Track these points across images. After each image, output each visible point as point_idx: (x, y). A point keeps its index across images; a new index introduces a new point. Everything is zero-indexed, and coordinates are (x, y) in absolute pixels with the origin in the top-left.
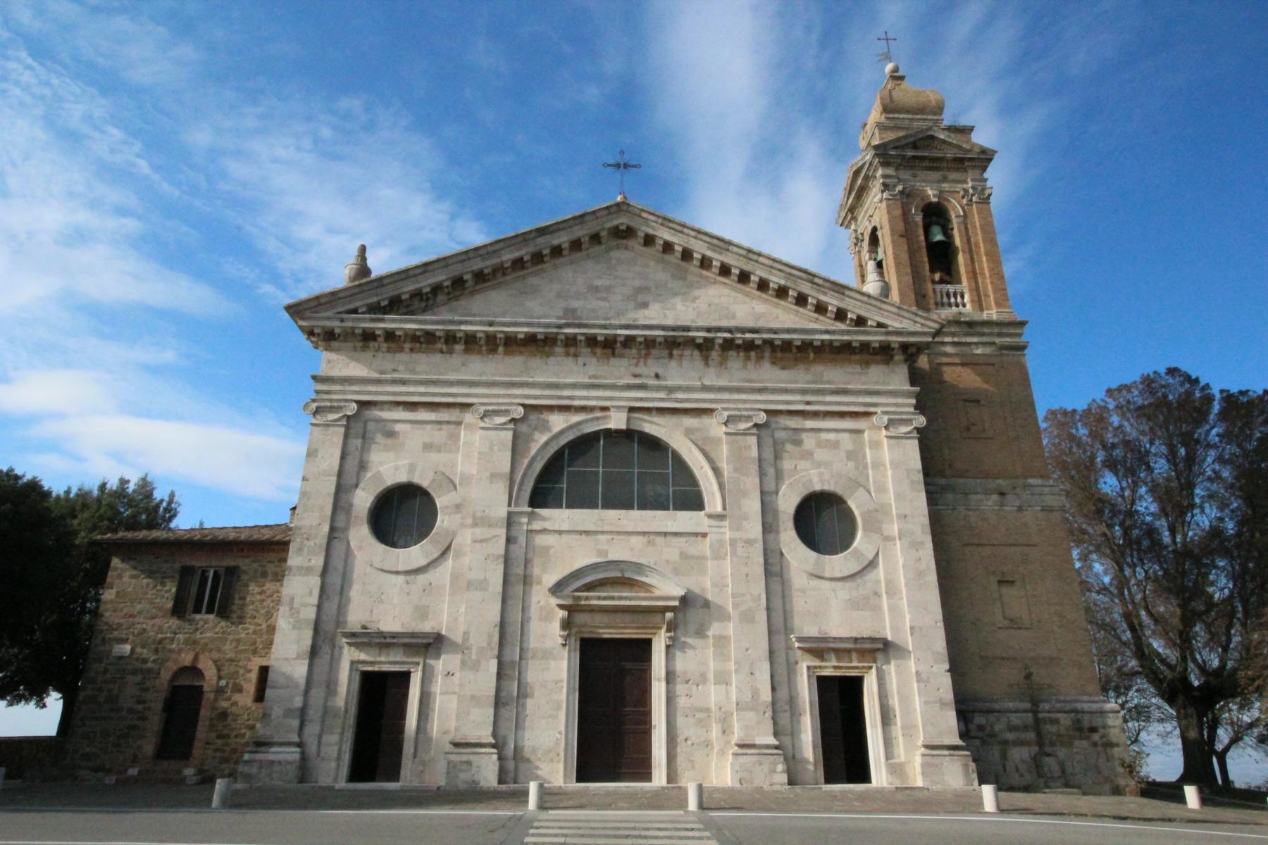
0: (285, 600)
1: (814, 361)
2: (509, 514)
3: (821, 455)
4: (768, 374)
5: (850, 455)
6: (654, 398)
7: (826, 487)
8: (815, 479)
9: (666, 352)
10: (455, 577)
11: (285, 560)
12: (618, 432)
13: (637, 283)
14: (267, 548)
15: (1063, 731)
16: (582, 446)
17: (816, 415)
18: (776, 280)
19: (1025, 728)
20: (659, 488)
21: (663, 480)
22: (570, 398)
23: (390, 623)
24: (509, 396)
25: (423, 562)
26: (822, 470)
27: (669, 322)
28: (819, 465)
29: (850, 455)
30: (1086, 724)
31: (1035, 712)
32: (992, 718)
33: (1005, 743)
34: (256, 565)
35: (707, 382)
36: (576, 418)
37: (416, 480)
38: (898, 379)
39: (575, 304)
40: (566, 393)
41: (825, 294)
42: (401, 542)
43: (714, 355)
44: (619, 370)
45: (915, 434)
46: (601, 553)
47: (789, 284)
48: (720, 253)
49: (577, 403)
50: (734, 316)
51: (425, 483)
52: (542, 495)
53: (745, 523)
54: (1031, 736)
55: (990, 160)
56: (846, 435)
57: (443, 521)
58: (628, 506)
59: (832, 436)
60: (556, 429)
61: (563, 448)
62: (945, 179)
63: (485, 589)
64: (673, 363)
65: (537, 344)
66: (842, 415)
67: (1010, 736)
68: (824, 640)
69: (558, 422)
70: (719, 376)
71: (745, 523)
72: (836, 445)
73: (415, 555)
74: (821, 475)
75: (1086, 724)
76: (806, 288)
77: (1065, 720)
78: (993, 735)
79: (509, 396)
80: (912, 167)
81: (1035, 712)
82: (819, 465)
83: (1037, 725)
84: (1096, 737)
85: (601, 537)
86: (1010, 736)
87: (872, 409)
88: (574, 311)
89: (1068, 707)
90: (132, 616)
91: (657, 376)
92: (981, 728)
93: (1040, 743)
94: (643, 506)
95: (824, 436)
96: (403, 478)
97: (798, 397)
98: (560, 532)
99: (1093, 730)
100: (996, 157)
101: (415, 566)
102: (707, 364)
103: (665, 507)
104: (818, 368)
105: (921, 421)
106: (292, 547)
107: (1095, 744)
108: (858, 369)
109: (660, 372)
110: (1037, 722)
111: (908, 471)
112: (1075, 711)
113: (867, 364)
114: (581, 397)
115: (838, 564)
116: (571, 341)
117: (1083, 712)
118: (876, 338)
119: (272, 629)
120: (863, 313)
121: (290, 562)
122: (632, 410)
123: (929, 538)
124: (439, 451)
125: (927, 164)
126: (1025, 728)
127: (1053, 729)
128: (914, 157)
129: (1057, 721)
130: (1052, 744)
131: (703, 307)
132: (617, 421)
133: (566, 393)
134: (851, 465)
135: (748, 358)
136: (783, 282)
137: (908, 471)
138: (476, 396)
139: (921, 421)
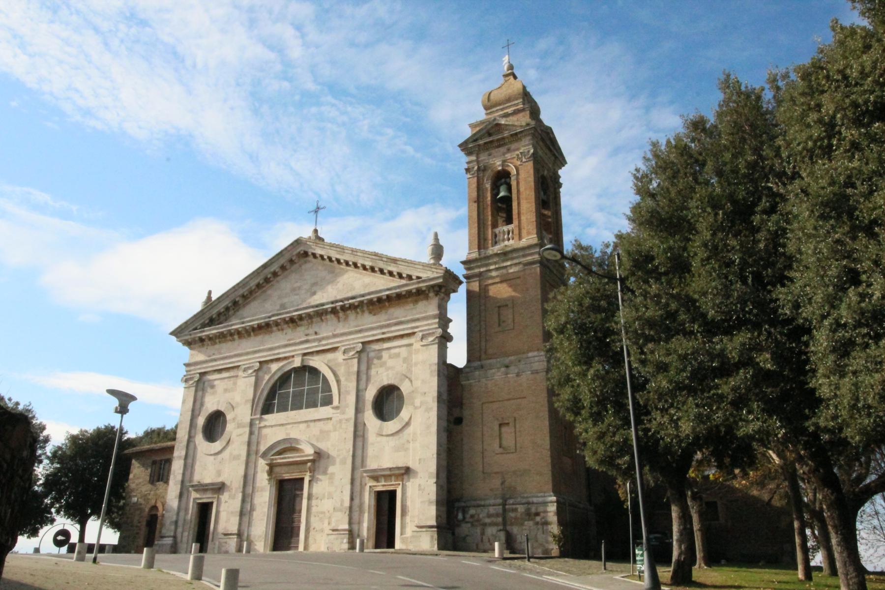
1: (389, 306)
2: (252, 420)
4: (368, 320)
5: (405, 360)
6: (313, 346)
8: (385, 379)
9: (319, 319)
10: (231, 454)
12: (299, 367)
17: (389, 339)
23: (207, 480)
29: (405, 360)
35: (338, 331)
36: (281, 364)
40: (276, 352)
43: (341, 314)
44: (299, 334)
49: (281, 356)
52: (267, 409)
61: (277, 381)
64: (324, 324)
65: (264, 328)
66: (402, 336)
69: (274, 367)
87: (416, 330)
91: (316, 333)
95: (393, 351)
98: (272, 426)
101: (217, 451)
102: (339, 321)
108: (411, 305)
109: (317, 330)
111: (430, 365)
113: (416, 302)
114: (283, 352)
122: (305, 354)
123: (436, 404)
132: (297, 363)
133: (276, 352)
134: (405, 365)
135: (357, 313)
137: (430, 365)
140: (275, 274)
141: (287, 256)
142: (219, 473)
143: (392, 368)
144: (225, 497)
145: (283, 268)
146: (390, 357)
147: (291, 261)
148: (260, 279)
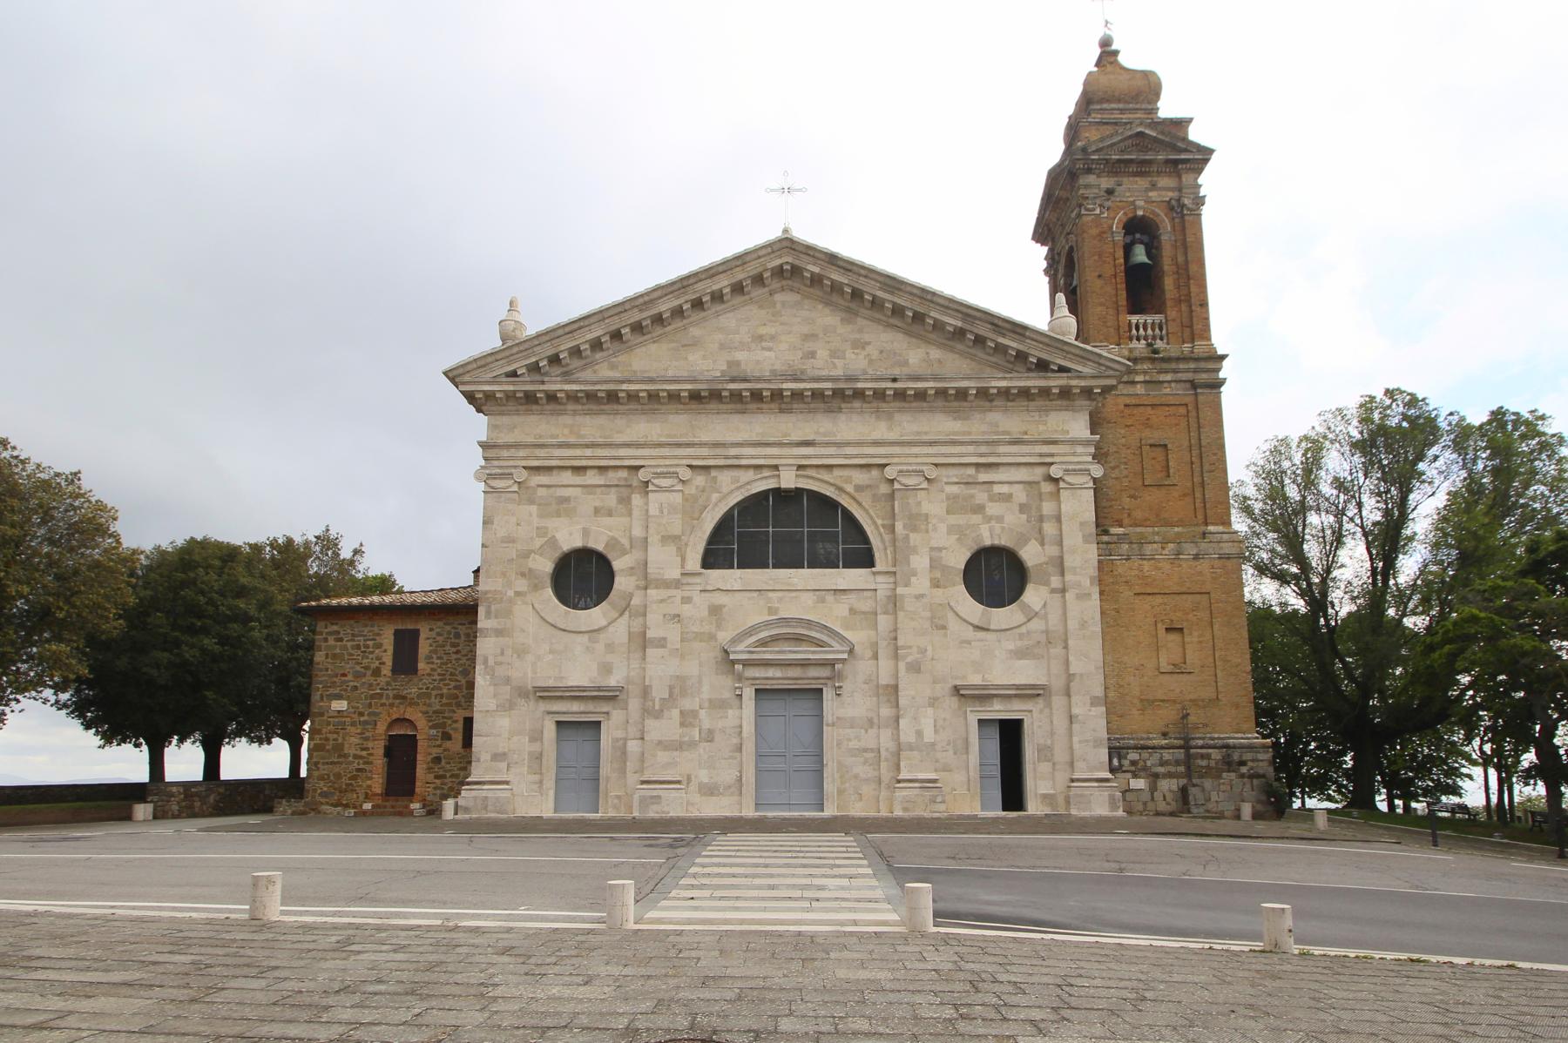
0: (479, 660)
3: (993, 509)
4: (941, 424)
5: (1023, 508)
7: (996, 542)
11: (475, 622)
13: (806, 330)
14: (458, 613)
15: (1213, 764)
16: (753, 507)
18: (953, 322)
19: (1177, 763)
20: (828, 546)
21: (833, 538)
22: (736, 457)
24: (676, 457)
25: (604, 623)
26: (993, 523)
27: (839, 372)
28: (989, 519)
29: (1023, 508)
30: (1236, 757)
31: (1186, 747)
32: (1145, 754)
33: (1156, 776)
34: (448, 628)
37: (592, 545)
38: (1077, 426)
39: (740, 356)
40: (733, 451)
41: (1004, 336)
42: (582, 603)
45: (1091, 484)
46: (771, 611)
47: (968, 327)
48: (892, 293)
50: (906, 363)
51: (600, 547)
52: (712, 559)
53: (913, 579)
54: (1182, 769)
55: (1206, 161)
56: (1021, 486)
57: (621, 583)
58: (798, 565)
59: (1005, 489)
60: (725, 490)
61: (732, 508)
62: (1153, 186)
63: (664, 646)
67: (1161, 770)
68: (985, 687)
70: (890, 429)
71: (913, 579)
72: (1007, 498)
73: (596, 616)
74: (991, 530)
75: (1236, 757)
76: (983, 330)
77: (1216, 755)
78: (1145, 769)
79: (676, 457)
80: (1116, 174)
81: (1186, 747)
82: (989, 519)
83: (1188, 761)
84: (1244, 770)
85: (771, 594)
86: (1161, 770)
88: (738, 363)
89: (1220, 742)
90: (344, 675)
92: (1133, 763)
93: (1189, 774)
94: (813, 565)
95: (997, 489)
96: (578, 544)
97: (971, 449)
99: (1243, 763)
100: (1214, 157)
103: (833, 565)
104: (995, 416)
105: (1098, 471)
106: (481, 611)
107: (1242, 776)
110: (1188, 755)
112: (1227, 747)
113: (1047, 411)
114: (752, 455)
115: (1003, 616)
116: (736, 396)
117: (1234, 747)
118: (1055, 382)
119: (471, 685)
120: (1044, 356)
121: (480, 625)
122: (800, 467)
124: (610, 515)
125: (1133, 168)
126: (1177, 763)
127: (1204, 763)
128: (1119, 161)
129: (1208, 756)
130: (1201, 777)
131: (875, 355)
132: (788, 480)
133: (733, 451)
134: (1024, 517)
136: (959, 324)
137: (1082, 524)
138: (643, 458)
139: (1098, 471)
140: (718, 297)
141: (753, 269)
142: (607, 669)
143: (1000, 519)
144: (617, 715)
145: (738, 288)
146: (992, 499)
147: (758, 280)
148: (683, 300)
